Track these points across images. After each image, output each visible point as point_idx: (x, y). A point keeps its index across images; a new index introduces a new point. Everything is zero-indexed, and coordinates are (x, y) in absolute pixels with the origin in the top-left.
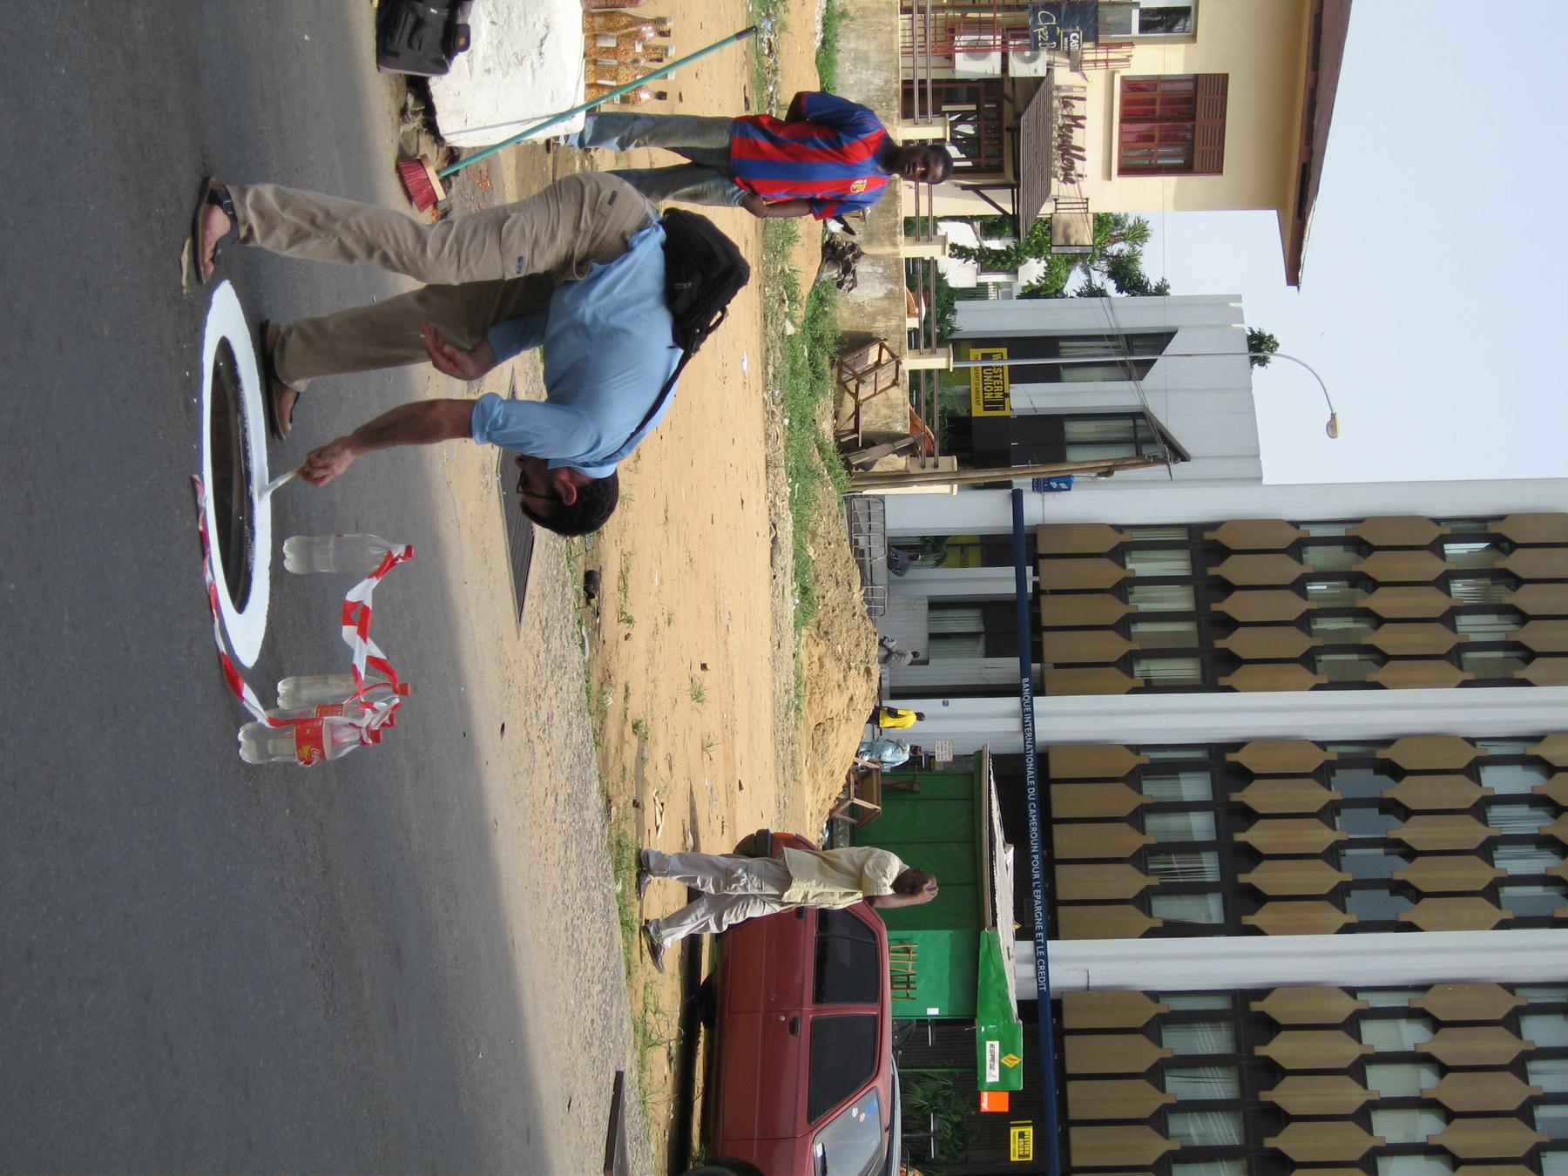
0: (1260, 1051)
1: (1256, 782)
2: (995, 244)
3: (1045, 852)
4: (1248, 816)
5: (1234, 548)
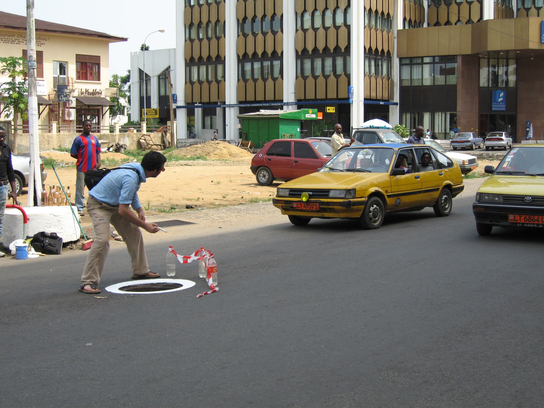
0: (321, 52)
1: (339, 45)
2: (311, 115)
3: (270, 102)
4: (326, 49)
5: (217, 54)
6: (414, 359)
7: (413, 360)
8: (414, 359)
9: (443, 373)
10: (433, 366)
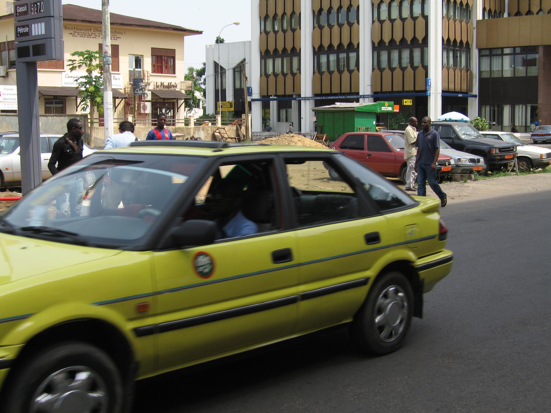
6: (470, 347)
7: (469, 348)
8: (470, 347)
9: (497, 361)
10: (488, 354)
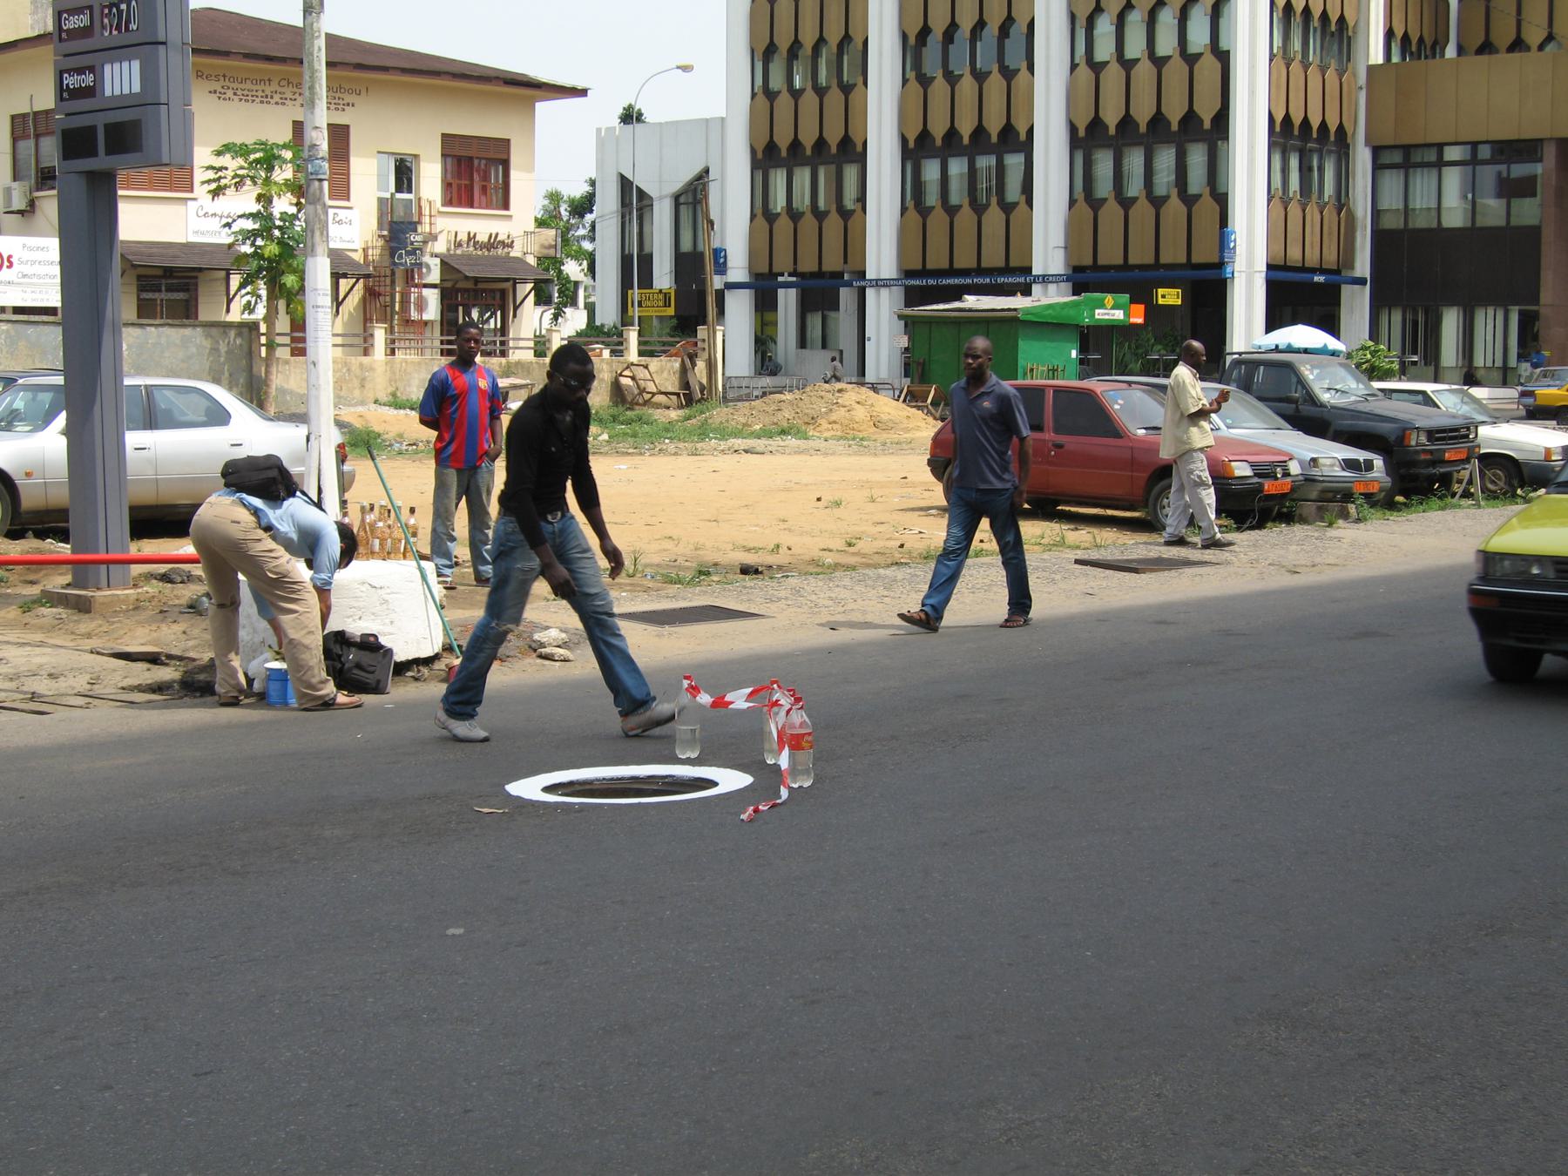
6: (1338, 994)
7: (1336, 998)
8: (1338, 994)
9: (1417, 1034)
10: (1389, 1016)
